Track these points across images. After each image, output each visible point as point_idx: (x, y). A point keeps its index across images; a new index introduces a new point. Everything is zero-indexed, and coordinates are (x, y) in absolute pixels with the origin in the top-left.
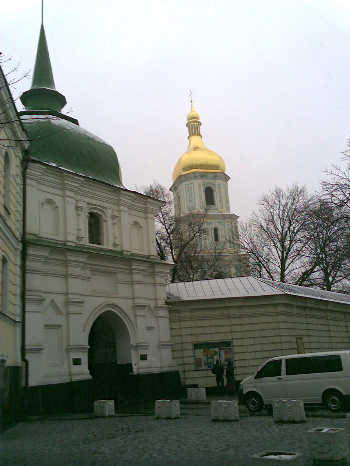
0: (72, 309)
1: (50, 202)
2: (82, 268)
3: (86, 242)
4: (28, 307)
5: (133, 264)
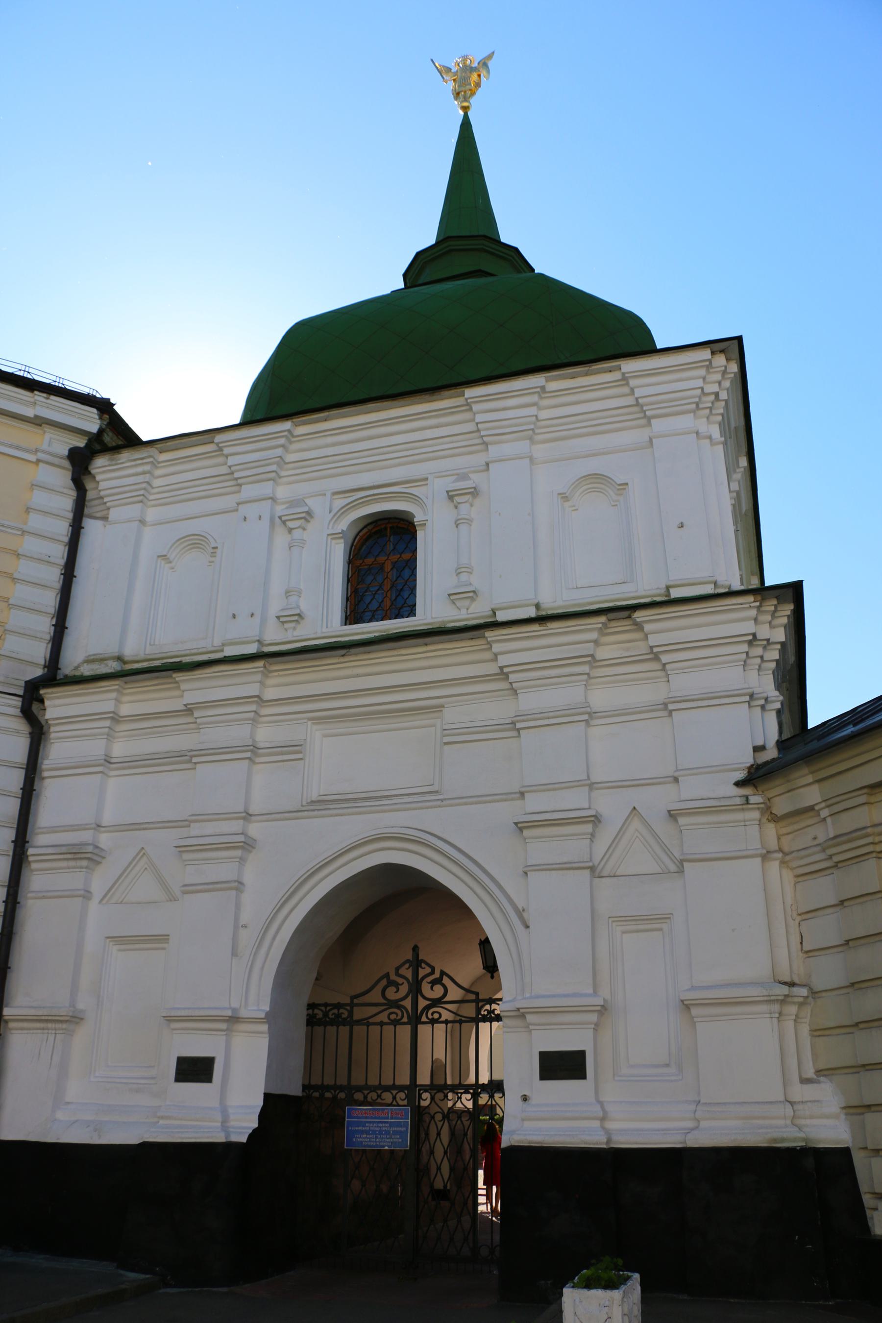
1: (196, 542)
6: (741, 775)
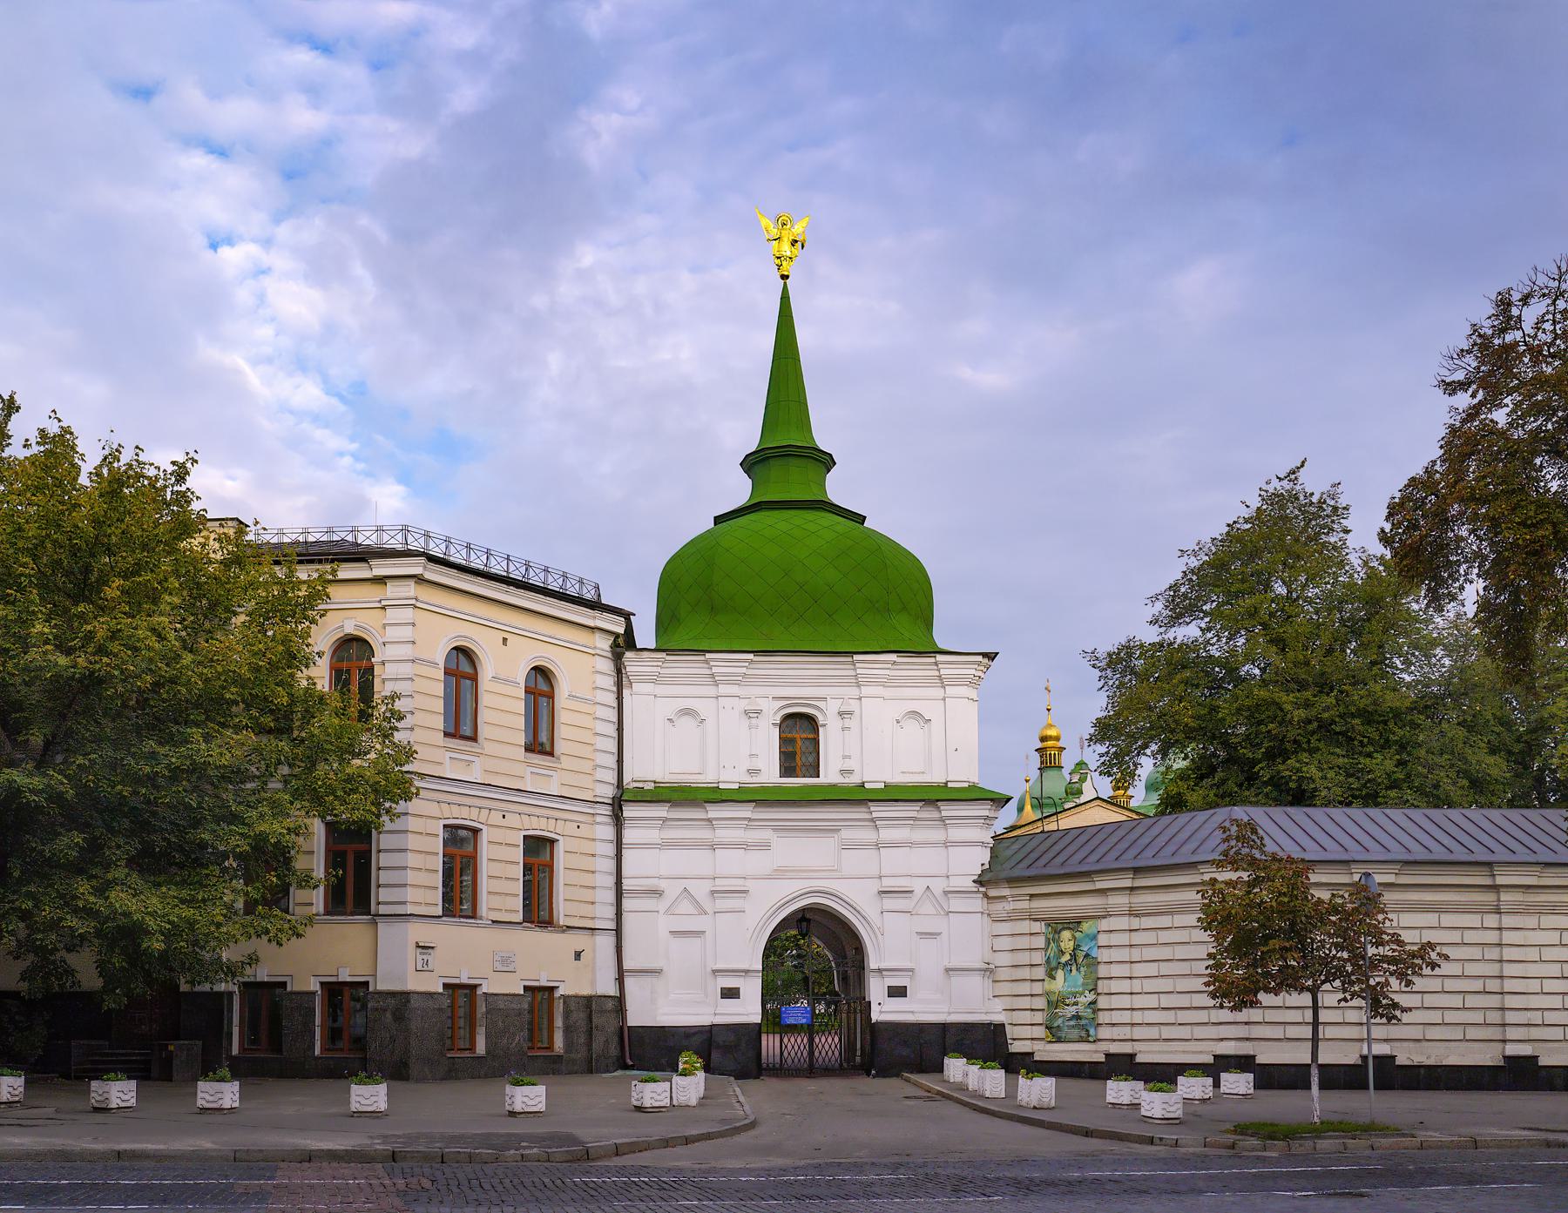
0: (723, 904)
1: (688, 712)
2: (747, 828)
3: (770, 773)
4: (627, 904)
5: (872, 809)
6: (976, 877)
